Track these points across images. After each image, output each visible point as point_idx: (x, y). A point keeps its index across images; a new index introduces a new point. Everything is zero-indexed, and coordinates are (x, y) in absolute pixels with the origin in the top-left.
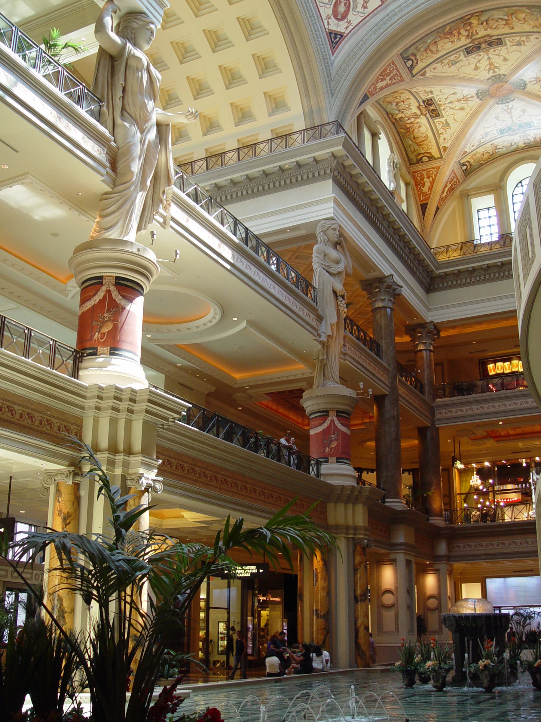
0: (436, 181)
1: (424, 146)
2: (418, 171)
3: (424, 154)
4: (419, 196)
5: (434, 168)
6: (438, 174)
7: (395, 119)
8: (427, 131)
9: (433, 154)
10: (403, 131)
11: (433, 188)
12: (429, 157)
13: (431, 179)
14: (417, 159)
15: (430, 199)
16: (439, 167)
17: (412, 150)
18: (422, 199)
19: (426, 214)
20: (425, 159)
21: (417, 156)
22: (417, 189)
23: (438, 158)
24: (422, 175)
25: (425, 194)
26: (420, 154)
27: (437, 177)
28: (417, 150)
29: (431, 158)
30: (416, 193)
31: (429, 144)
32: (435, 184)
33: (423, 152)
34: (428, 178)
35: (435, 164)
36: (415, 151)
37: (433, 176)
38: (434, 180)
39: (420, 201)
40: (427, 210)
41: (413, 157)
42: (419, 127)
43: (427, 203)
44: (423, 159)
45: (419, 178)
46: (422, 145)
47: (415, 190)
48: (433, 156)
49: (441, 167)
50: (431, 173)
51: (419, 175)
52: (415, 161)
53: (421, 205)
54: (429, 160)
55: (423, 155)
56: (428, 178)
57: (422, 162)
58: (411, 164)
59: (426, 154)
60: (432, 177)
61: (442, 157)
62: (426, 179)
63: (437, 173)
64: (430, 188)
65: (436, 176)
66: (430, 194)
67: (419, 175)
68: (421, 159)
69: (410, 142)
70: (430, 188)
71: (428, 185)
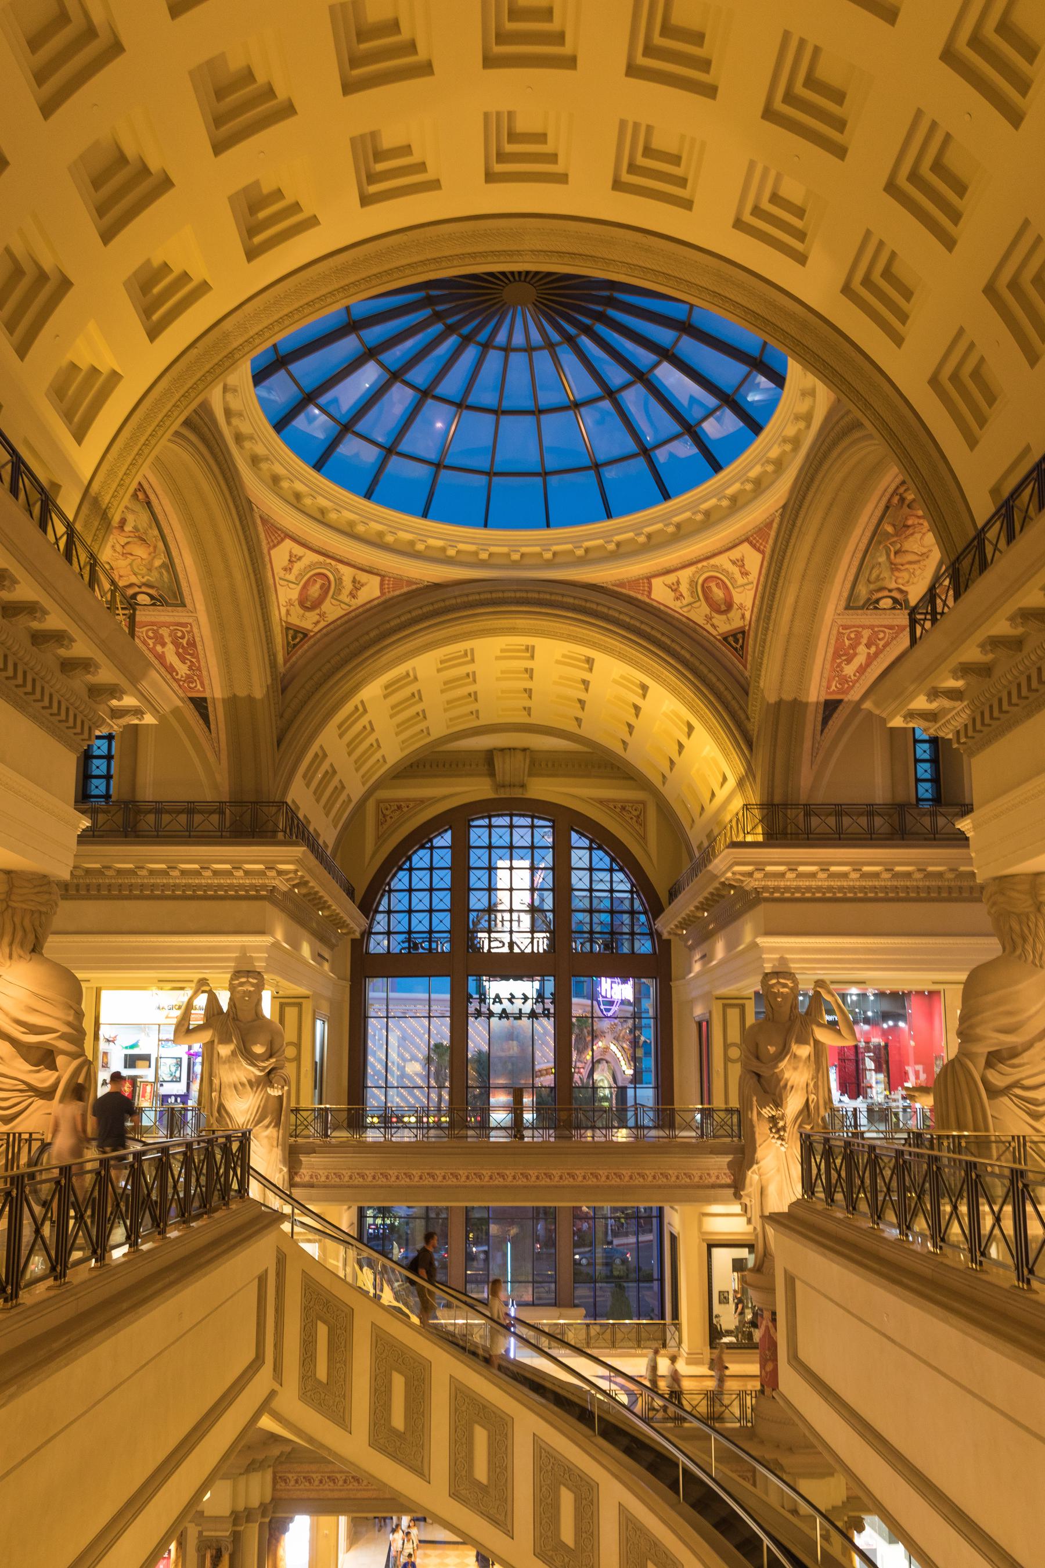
0: (882, 656)
2: (854, 626)
3: (890, 591)
5: (890, 627)
7: (902, 500)
11: (869, 670)
12: (895, 601)
13: (873, 649)
14: (869, 599)
18: (833, 688)
21: (871, 592)
22: (832, 666)
24: (859, 636)
25: (844, 680)
27: (888, 649)
28: (883, 579)
31: (918, 572)
32: (875, 663)
33: (893, 585)
34: (868, 646)
36: (878, 579)
37: (881, 643)
39: (827, 693)
45: (847, 642)
47: (828, 666)
50: (881, 635)
51: (853, 636)
52: (861, 603)
54: (894, 608)
55: (886, 593)
57: (876, 608)
58: (848, 607)
60: (877, 646)
62: (862, 649)
63: (893, 639)
65: (885, 646)
66: (857, 681)
67: (853, 636)
68: (877, 601)
69: (882, 559)
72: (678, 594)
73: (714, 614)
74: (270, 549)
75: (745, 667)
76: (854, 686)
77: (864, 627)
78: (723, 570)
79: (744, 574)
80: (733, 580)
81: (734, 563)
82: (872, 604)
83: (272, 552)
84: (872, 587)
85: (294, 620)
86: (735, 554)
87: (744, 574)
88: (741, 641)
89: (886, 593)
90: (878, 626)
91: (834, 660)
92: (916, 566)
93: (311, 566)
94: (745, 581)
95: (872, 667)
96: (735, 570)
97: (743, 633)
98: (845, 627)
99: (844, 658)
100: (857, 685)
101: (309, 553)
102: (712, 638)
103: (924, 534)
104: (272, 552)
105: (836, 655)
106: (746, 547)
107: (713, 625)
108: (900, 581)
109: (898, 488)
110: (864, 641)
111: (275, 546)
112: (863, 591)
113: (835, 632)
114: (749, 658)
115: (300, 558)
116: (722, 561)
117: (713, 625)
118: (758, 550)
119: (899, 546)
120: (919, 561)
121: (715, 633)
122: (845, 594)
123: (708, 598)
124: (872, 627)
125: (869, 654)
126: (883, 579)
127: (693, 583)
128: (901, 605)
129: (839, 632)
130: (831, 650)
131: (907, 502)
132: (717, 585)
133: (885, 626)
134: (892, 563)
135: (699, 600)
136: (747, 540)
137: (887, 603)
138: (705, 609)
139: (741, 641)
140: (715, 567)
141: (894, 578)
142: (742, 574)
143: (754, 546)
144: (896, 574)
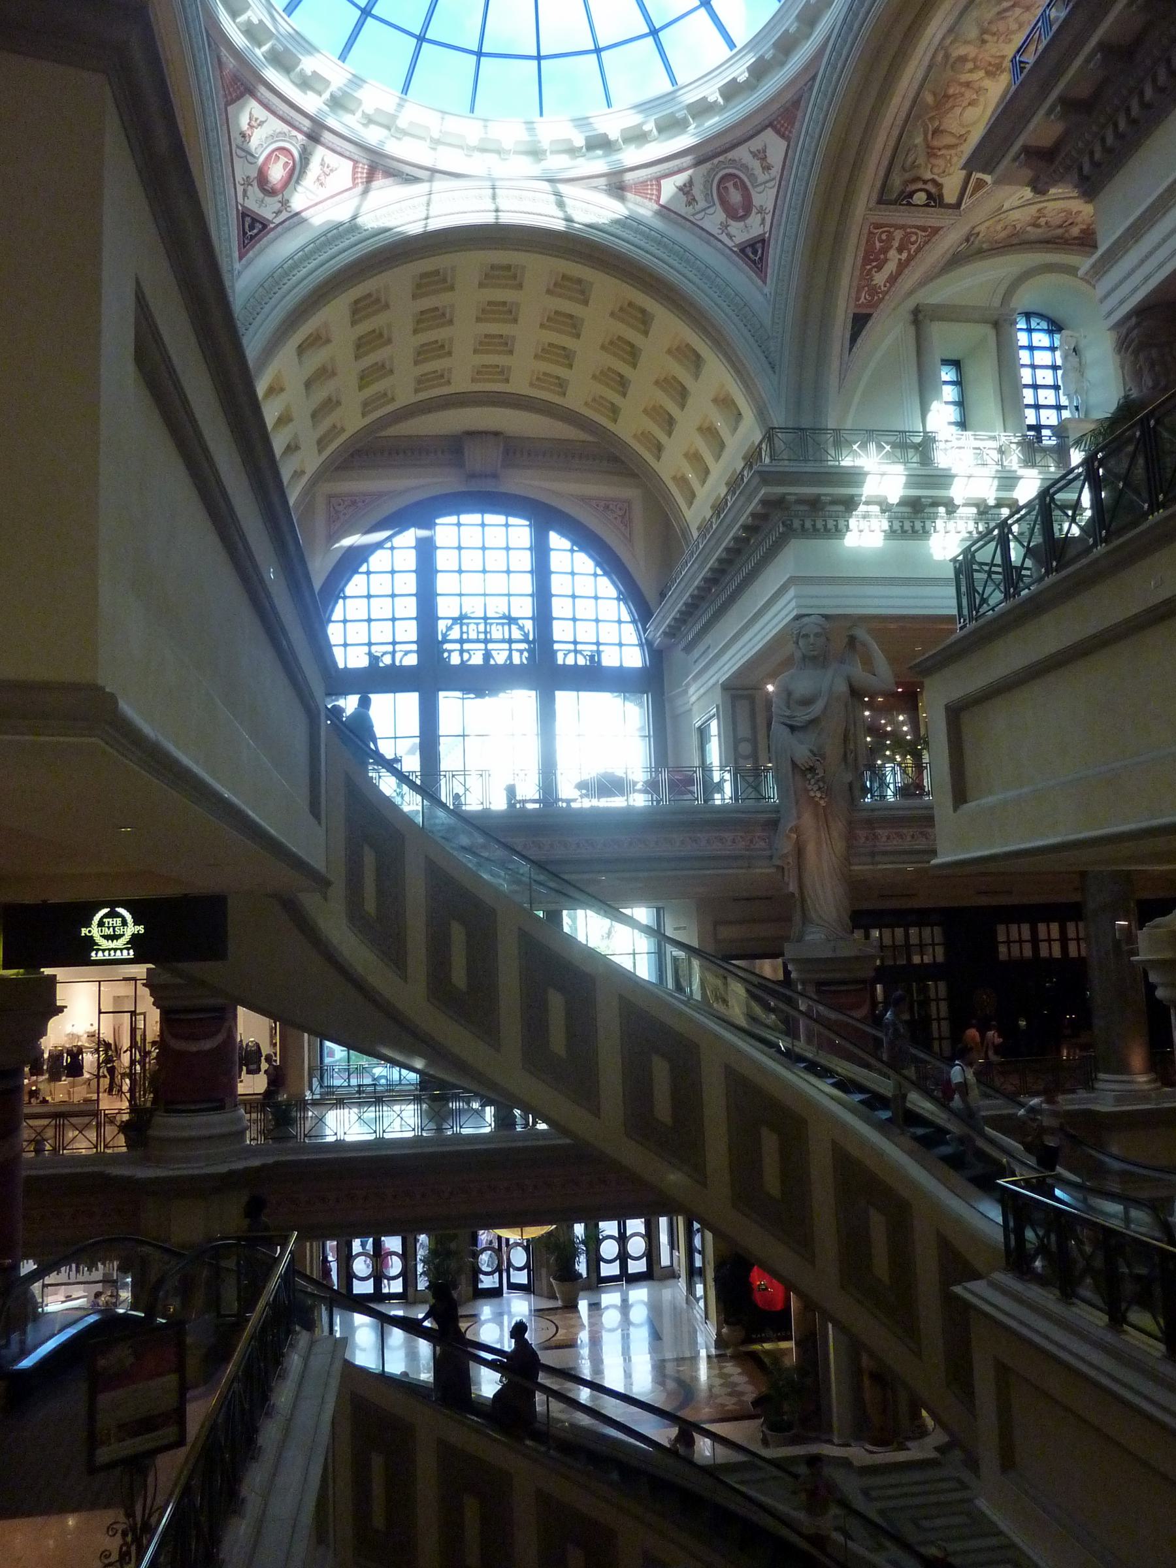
0: (913, 263)
1: (941, 162)
3: (925, 182)
4: (859, 292)
5: (924, 229)
6: (927, 247)
7: (947, 56)
8: (974, 123)
9: (945, 191)
10: (929, 99)
12: (930, 196)
13: (904, 255)
14: (903, 192)
15: (882, 306)
16: (936, 230)
17: (910, 160)
18: (862, 299)
19: (859, 341)
20: (920, 198)
21: (906, 183)
23: (949, 206)
24: (890, 237)
25: (874, 290)
26: (917, 179)
27: (919, 255)
28: (919, 167)
29: (935, 200)
30: (855, 284)
32: (906, 271)
33: (928, 176)
34: (900, 250)
35: (932, 218)
36: (914, 166)
37: (913, 248)
38: (910, 259)
40: (864, 333)
41: (897, 181)
42: (972, 103)
43: (869, 316)
44: (915, 197)
45: (878, 245)
46: (935, 155)
47: (857, 273)
48: (941, 196)
49: (941, 232)
50: (913, 239)
51: (884, 237)
53: (854, 314)
54: (927, 205)
55: (920, 185)
56: (900, 250)
57: (909, 204)
58: (880, 201)
59: (929, 187)
61: (958, 205)
62: (893, 254)
63: (926, 243)
64: (893, 279)
66: (887, 293)
67: (884, 237)
68: (911, 195)
69: (919, 140)
70: (893, 279)
71: (891, 267)
72: (690, 197)
73: (731, 222)
74: (227, 104)
75: (765, 282)
76: (883, 298)
77: (897, 227)
78: (742, 165)
79: (767, 168)
80: (753, 177)
81: (754, 155)
82: (905, 199)
83: (229, 108)
84: (907, 176)
85: (252, 204)
86: (756, 144)
87: (767, 168)
88: (760, 252)
89: (920, 185)
90: (910, 227)
91: (864, 264)
92: (953, 152)
93: (274, 137)
94: (767, 177)
95: (903, 276)
96: (756, 165)
97: (763, 241)
98: (877, 226)
99: (875, 264)
100: (887, 297)
101: (271, 117)
102: (728, 251)
103: (965, 108)
104: (229, 108)
105: (866, 260)
106: (769, 136)
107: (730, 237)
108: (936, 170)
109: (943, 39)
110: (896, 244)
111: (233, 101)
112: (897, 181)
113: (865, 231)
114: (769, 271)
115: (261, 124)
116: (742, 154)
117: (730, 237)
118: (783, 136)
119: (937, 123)
120: (957, 145)
121: (730, 244)
122: (878, 184)
123: (724, 202)
124: (903, 227)
125: (900, 260)
126: (919, 167)
127: (707, 183)
128: (935, 202)
129: (870, 233)
130: (861, 254)
131: (952, 60)
132: (735, 185)
133: (918, 227)
134: (928, 147)
135: (714, 204)
136: (770, 125)
137: (920, 198)
138: (719, 215)
139: (760, 252)
140: (733, 161)
141: (930, 166)
142: (763, 168)
143: (778, 132)
144: (933, 161)
